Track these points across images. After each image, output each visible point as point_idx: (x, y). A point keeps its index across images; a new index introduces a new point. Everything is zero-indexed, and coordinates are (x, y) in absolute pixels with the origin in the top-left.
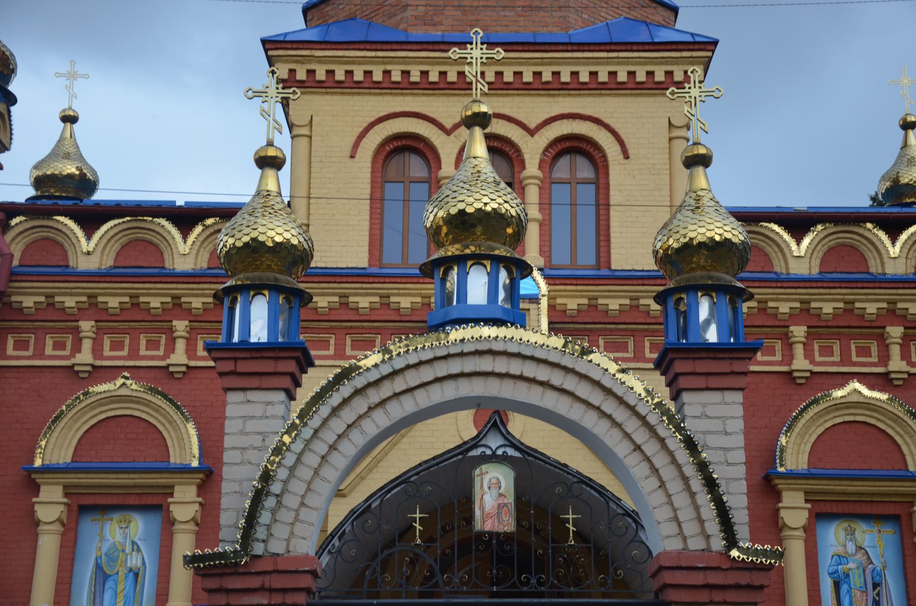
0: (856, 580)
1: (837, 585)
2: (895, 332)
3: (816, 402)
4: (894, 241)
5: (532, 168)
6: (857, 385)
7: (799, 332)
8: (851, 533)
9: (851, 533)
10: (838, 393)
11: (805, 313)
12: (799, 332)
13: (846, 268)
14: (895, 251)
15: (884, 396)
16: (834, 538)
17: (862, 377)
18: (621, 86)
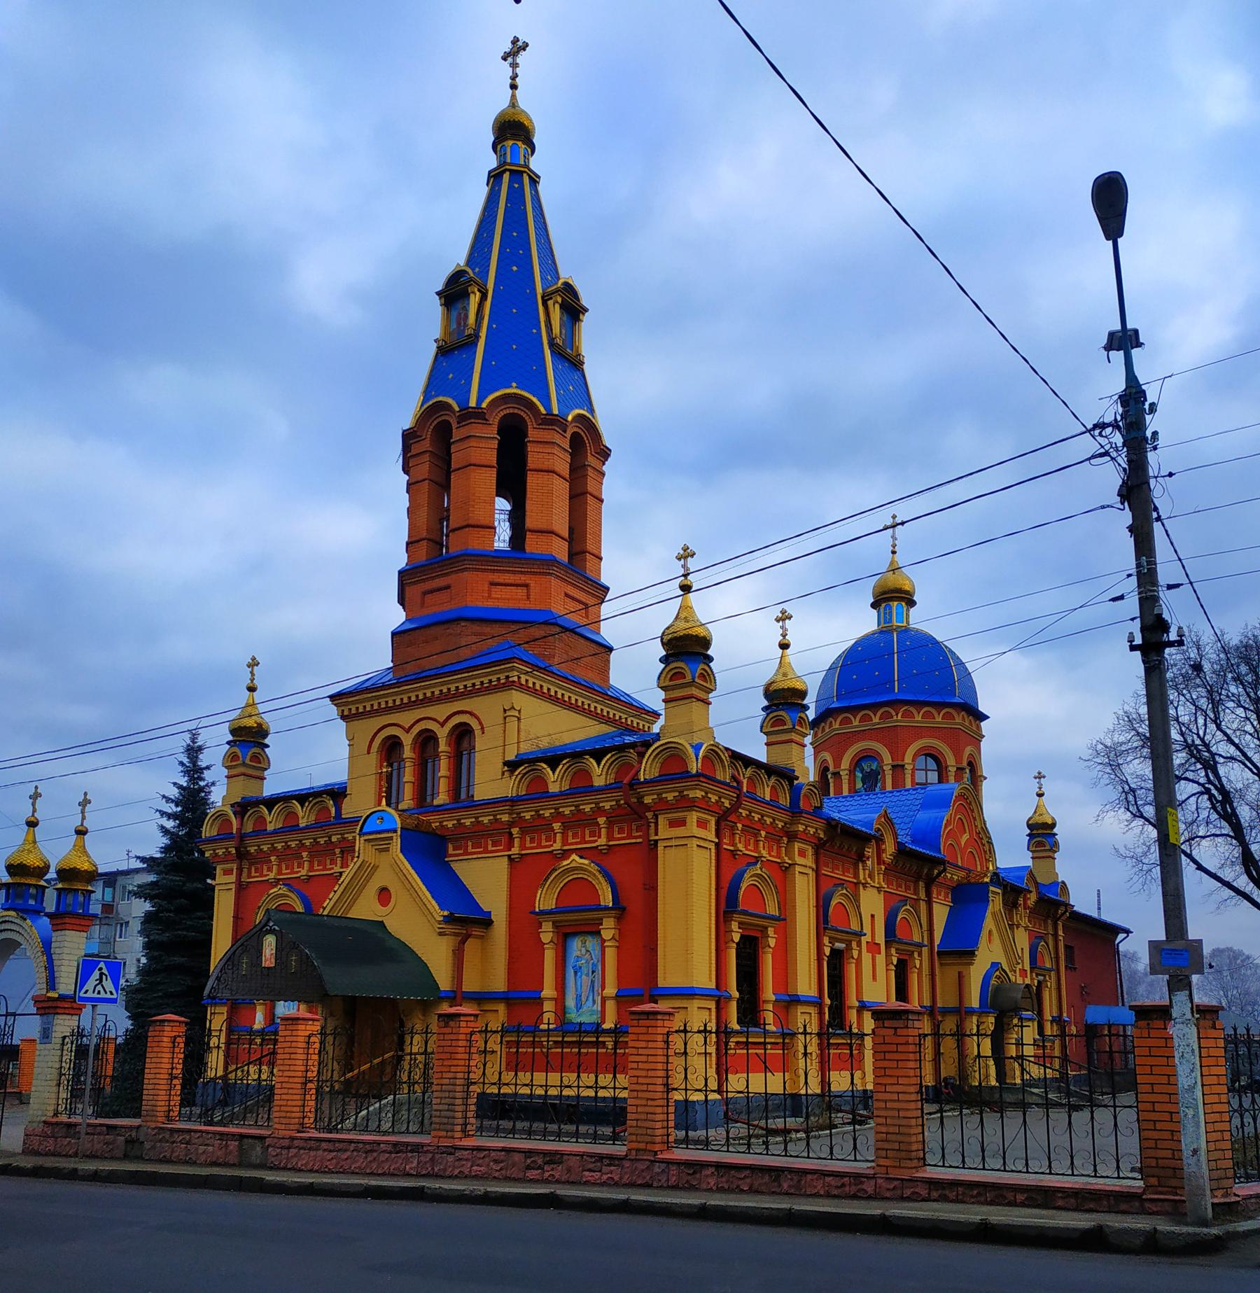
0: (585, 970)
1: (576, 973)
2: (601, 820)
3: (554, 870)
4: (599, 764)
5: (443, 746)
6: (574, 857)
7: (557, 826)
8: (584, 943)
9: (584, 943)
10: (565, 863)
11: (558, 816)
12: (557, 826)
13: (580, 786)
14: (598, 771)
15: (586, 862)
16: (576, 947)
17: (577, 851)
18: (479, 690)
